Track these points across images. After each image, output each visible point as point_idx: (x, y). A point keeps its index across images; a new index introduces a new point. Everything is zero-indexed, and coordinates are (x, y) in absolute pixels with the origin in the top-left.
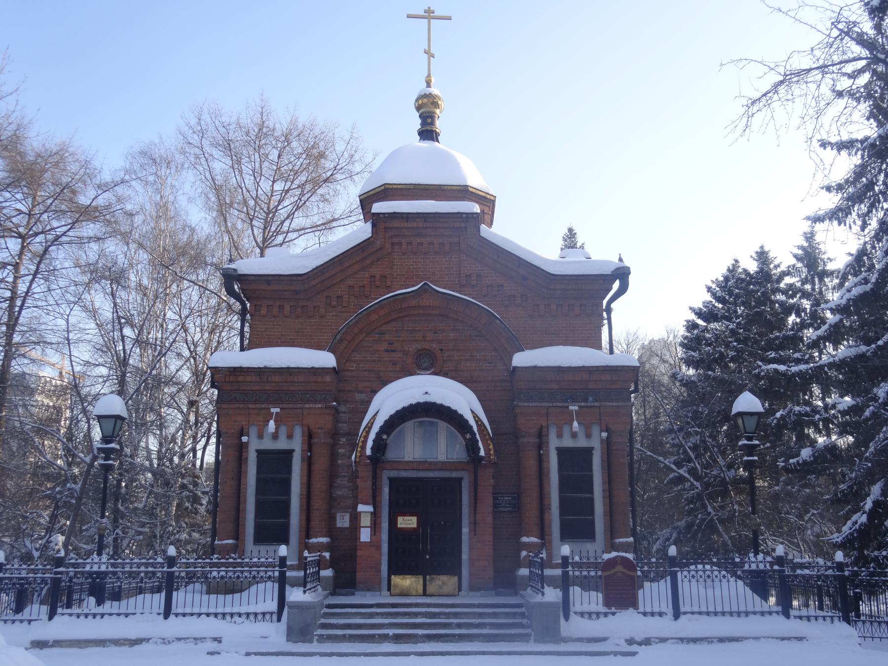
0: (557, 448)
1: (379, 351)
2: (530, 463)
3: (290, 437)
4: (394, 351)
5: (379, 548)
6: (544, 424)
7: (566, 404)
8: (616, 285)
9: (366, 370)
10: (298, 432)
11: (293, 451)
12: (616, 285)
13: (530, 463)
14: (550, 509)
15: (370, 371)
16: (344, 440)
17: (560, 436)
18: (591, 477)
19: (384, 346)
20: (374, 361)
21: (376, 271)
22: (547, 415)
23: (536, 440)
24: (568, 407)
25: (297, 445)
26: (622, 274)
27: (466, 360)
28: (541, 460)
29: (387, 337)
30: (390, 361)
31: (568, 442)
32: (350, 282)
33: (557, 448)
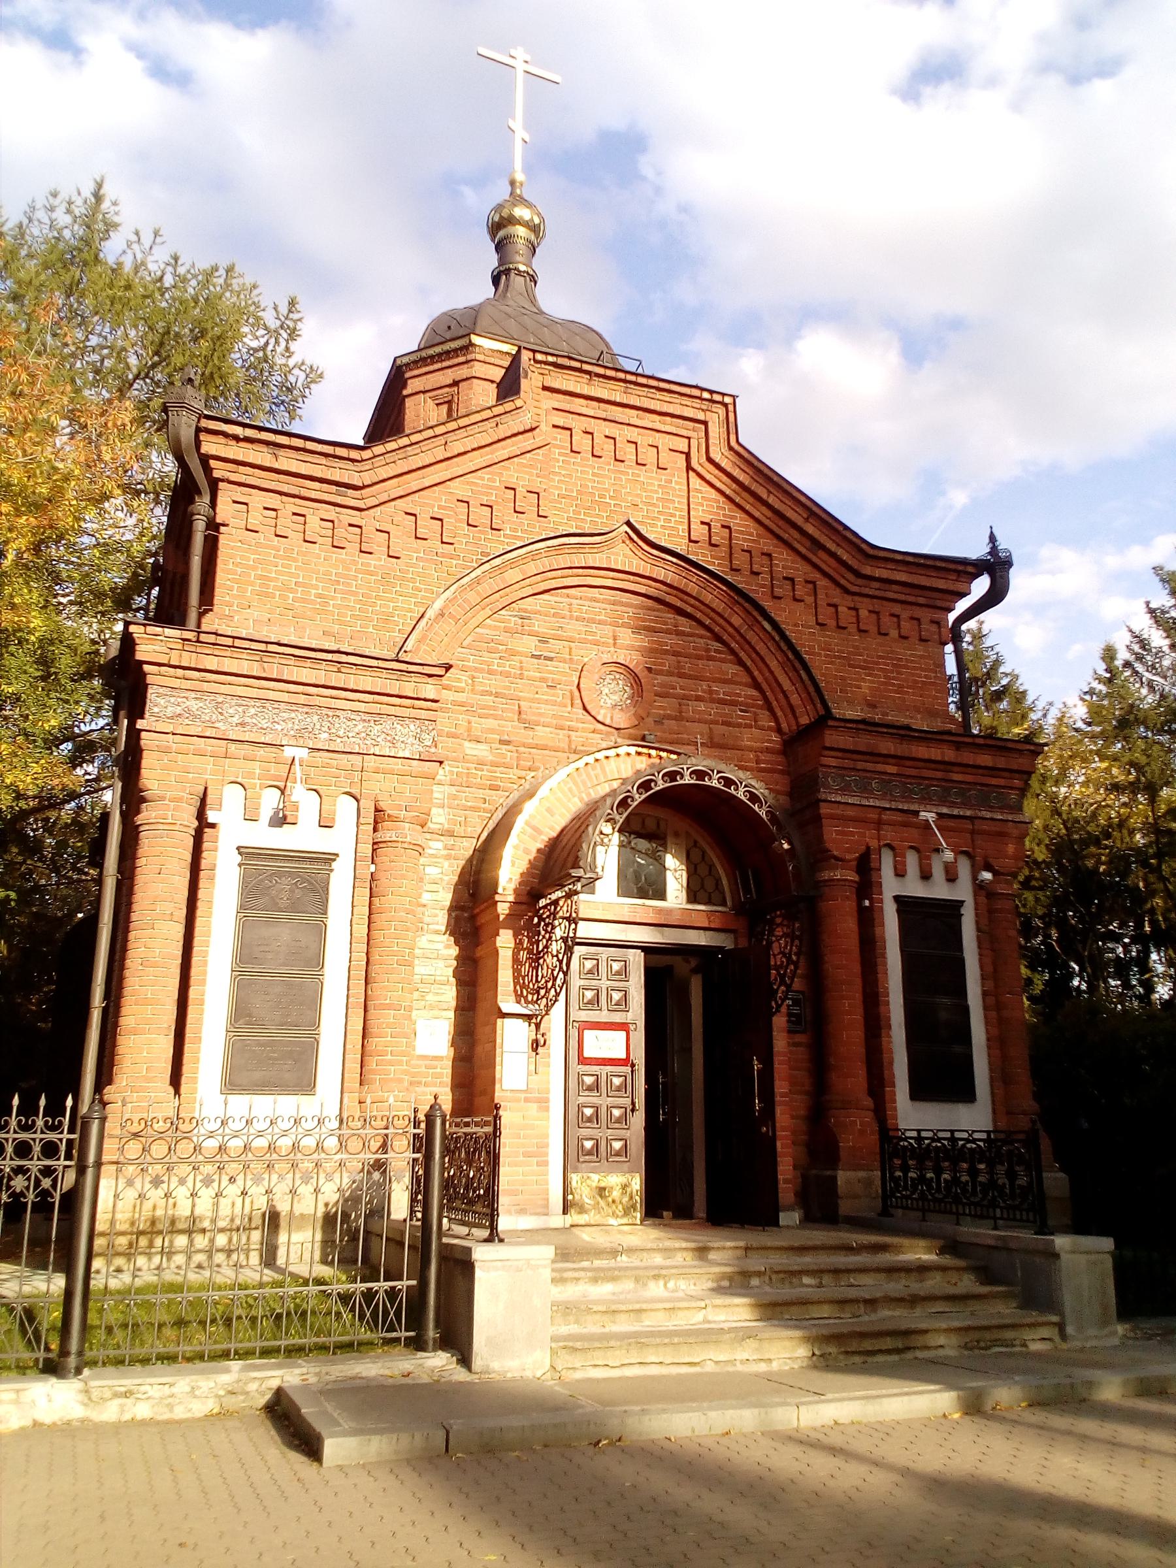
0: (897, 898)
1: (514, 653)
2: (845, 925)
3: (325, 824)
4: (551, 659)
5: (543, 1103)
6: (874, 844)
7: (914, 807)
8: (981, 586)
9: (491, 694)
10: (345, 809)
11: (328, 859)
12: (981, 586)
13: (845, 925)
14: (889, 1027)
15: (497, 695)
16: (440, 845)
17: (900, 873)
18: (962, 962)
19: (529, 644)
20: (507, 675)
21: (519, 475)
22: (879, 824)
23: (853, 876)
24: (916, 813)
25: (343, 840)
26: (997, 566)
27: (698, 699)
28: (868, 920)
29: (538, 626)
30: (543, 680)
31: (915, 888)
32: (459, 489)
33: (897, 898)
